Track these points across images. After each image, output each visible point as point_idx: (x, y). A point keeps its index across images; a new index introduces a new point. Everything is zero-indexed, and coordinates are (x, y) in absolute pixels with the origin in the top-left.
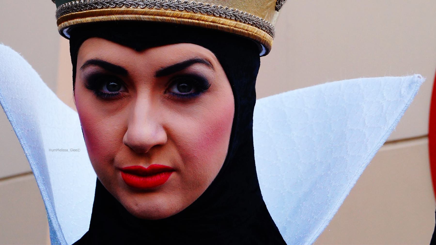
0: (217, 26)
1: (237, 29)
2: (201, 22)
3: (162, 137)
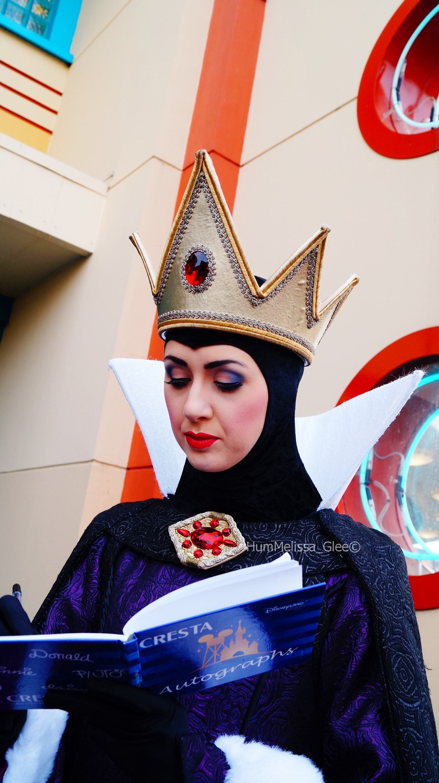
0: (251, 334)
1: (268, 337)
2: (238, 330)
3: (207, 412)
